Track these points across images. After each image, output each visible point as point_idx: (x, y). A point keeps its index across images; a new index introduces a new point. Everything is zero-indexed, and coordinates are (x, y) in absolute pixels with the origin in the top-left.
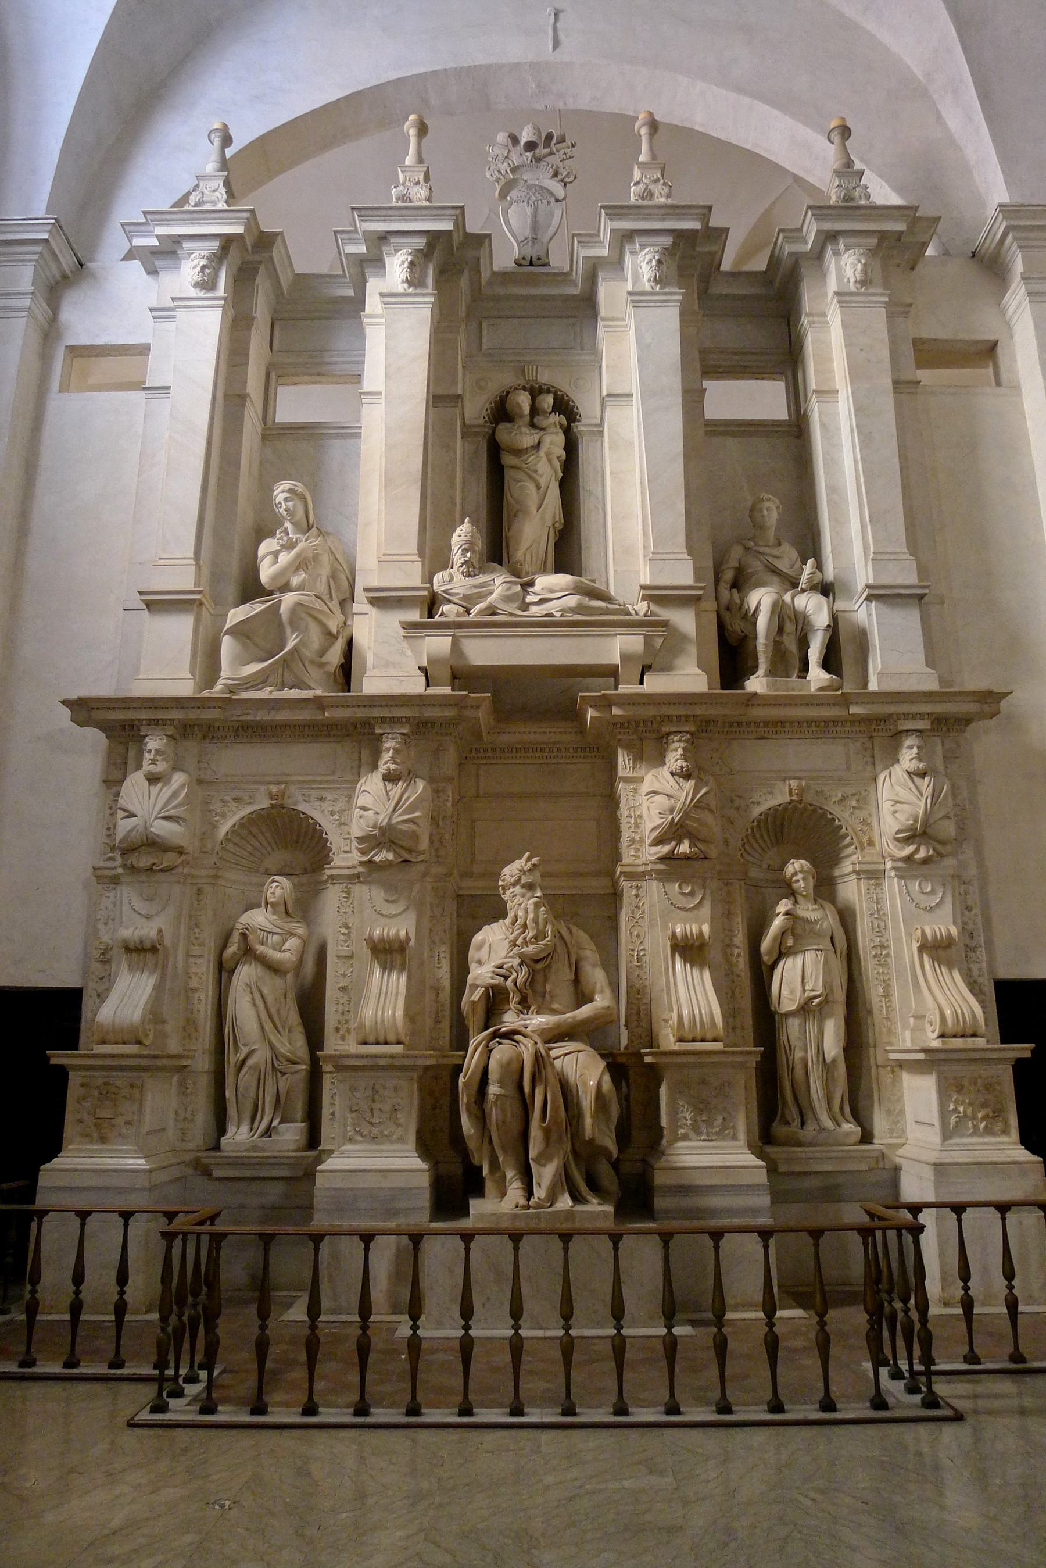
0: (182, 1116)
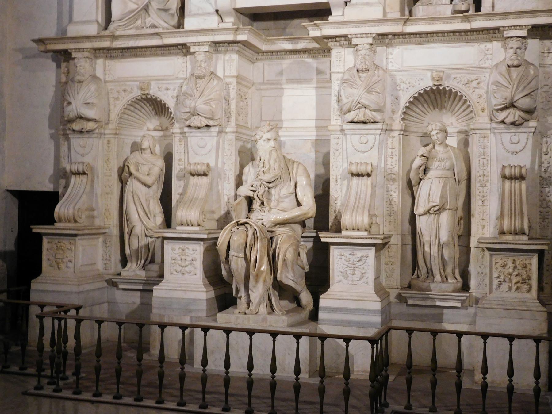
0: (105, 258)
